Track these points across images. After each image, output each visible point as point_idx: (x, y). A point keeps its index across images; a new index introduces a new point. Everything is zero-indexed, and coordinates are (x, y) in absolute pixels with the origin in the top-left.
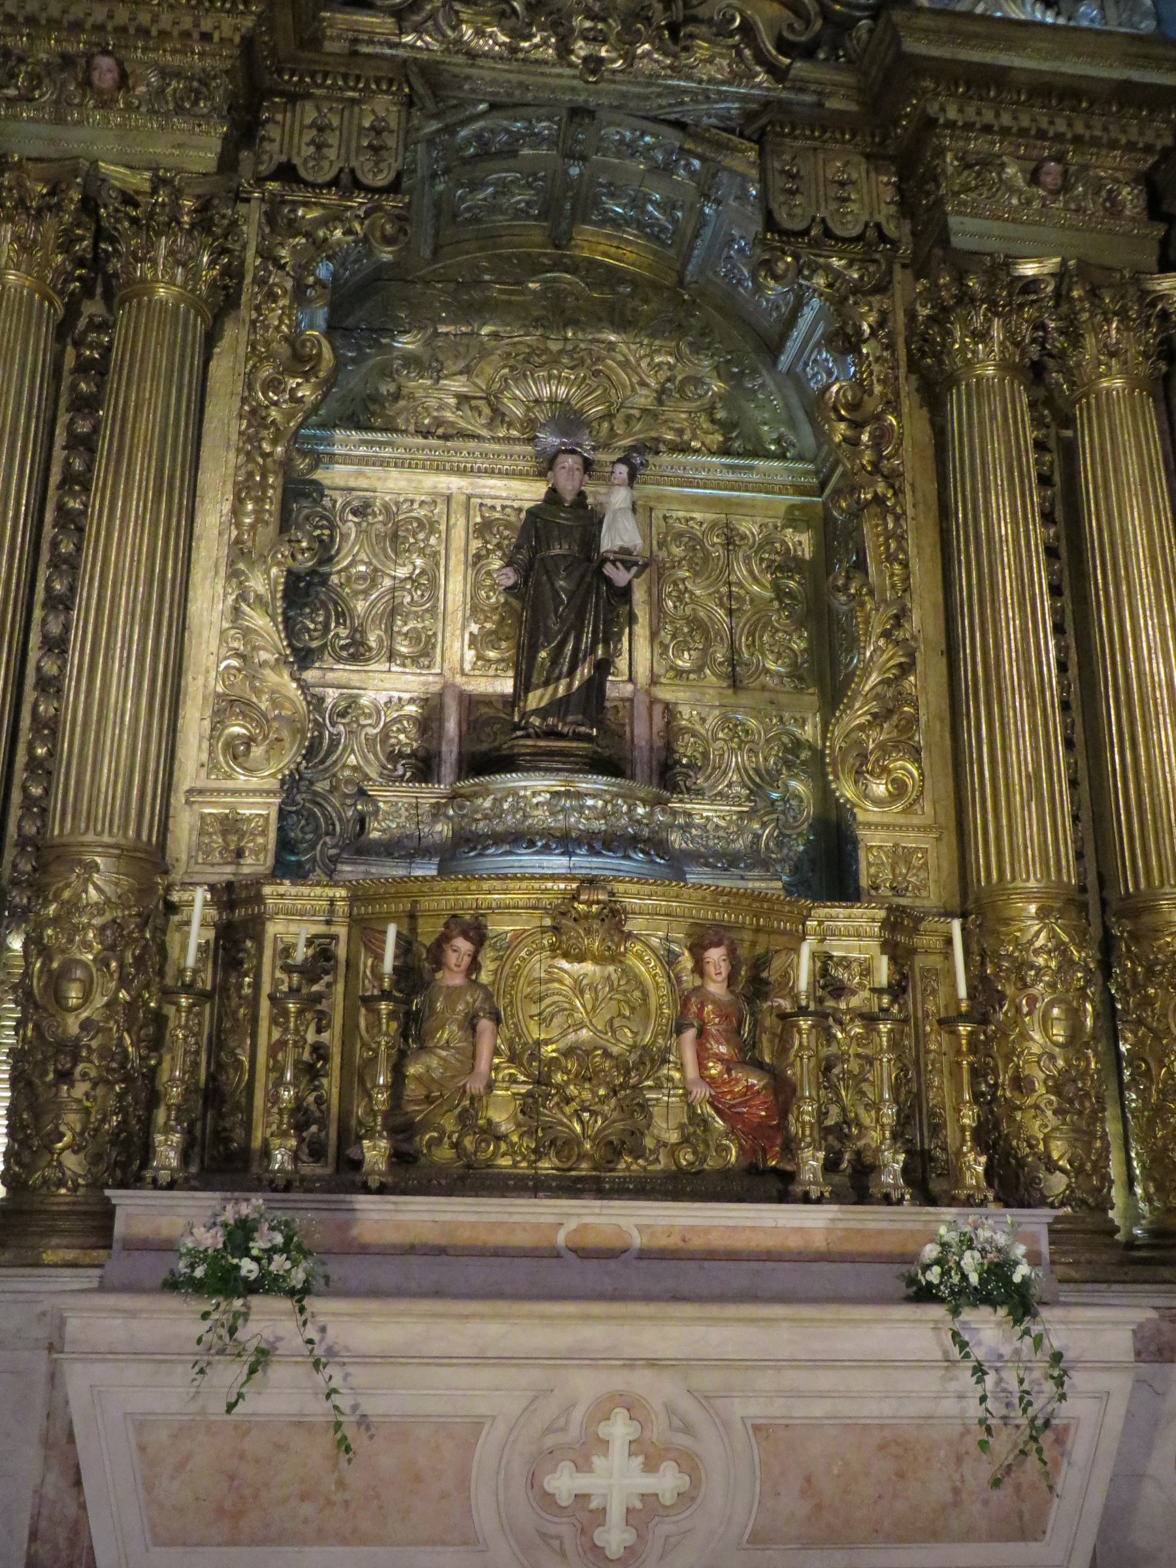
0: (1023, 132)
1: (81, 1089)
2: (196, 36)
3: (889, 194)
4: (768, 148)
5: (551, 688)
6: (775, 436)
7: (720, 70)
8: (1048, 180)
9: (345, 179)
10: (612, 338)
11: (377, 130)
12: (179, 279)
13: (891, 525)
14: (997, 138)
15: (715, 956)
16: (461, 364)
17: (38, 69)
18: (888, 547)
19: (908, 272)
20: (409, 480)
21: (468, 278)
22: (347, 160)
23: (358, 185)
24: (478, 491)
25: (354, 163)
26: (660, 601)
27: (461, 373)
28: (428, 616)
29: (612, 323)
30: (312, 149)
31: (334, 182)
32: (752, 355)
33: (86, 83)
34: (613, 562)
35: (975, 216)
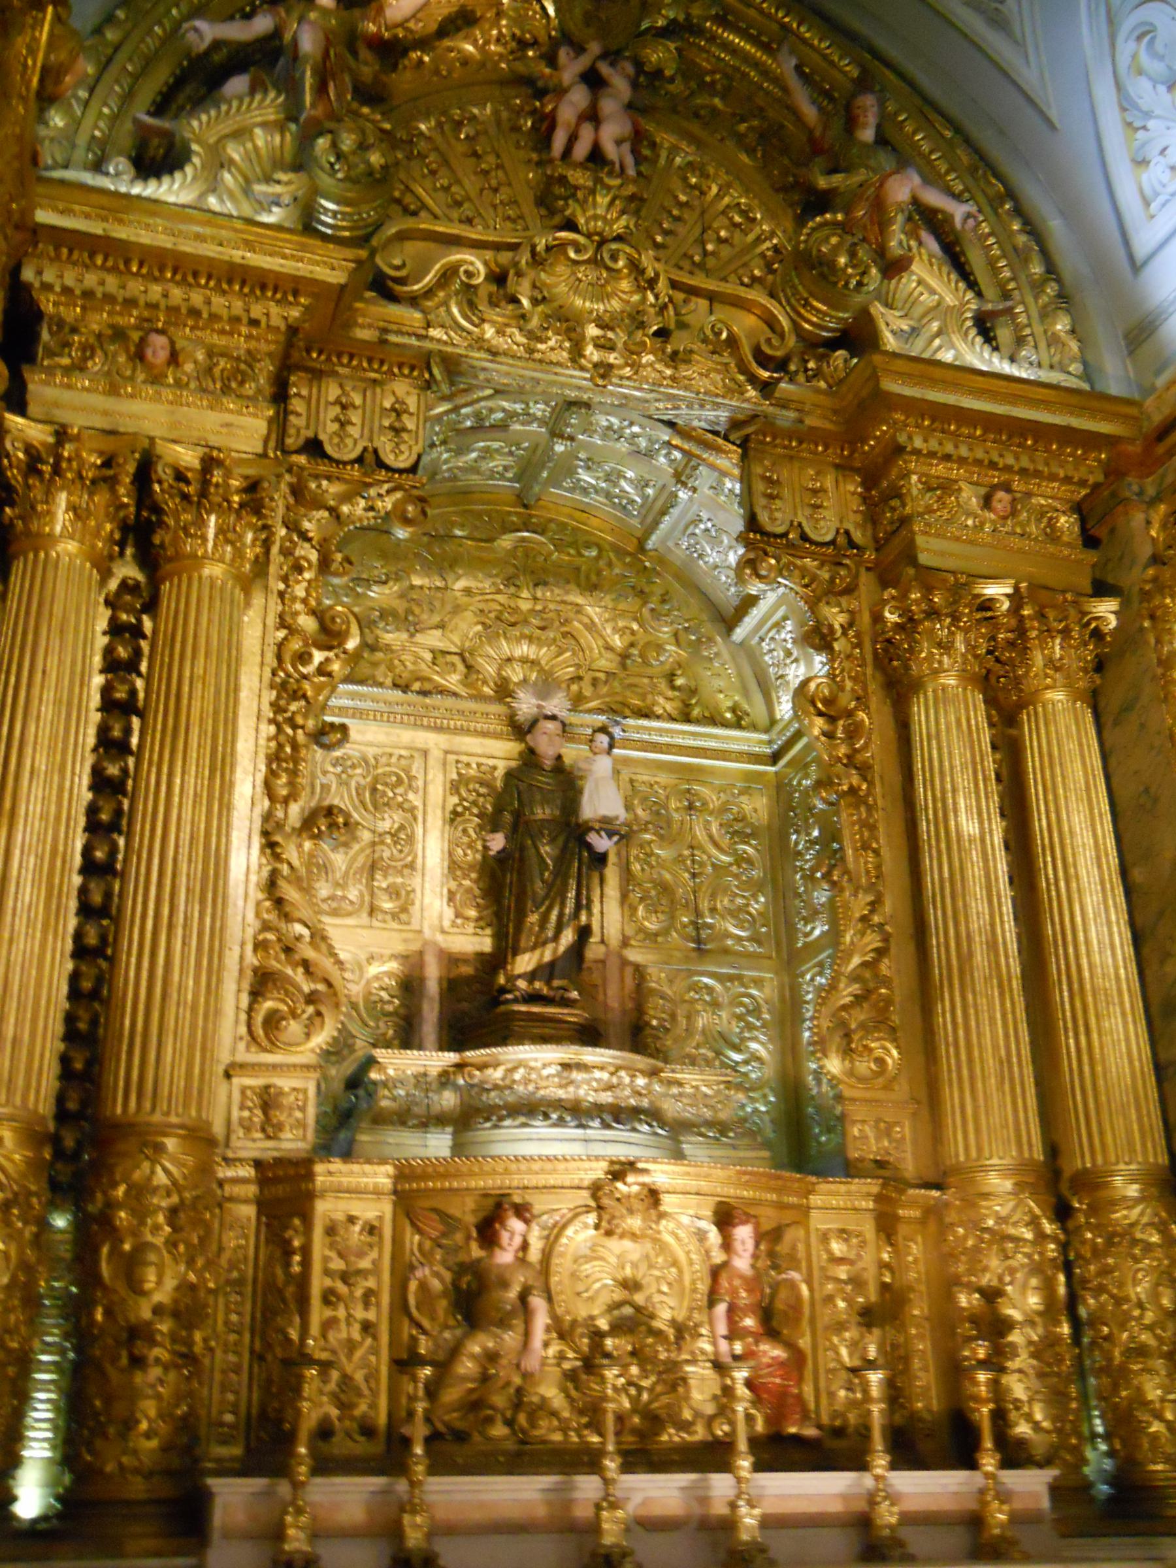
0: (978, 462)
1: (155, 1372)
2: (245, 320)
3: (855, 504)
4: (751, 453)
5: (537, 952)
6: (729, 704)
7: (714, 383)
8: (999, 506)
9: (370, 457)
10: (580, 600)
11: (398, 411)
12: (228, 557)
13: (864, 815)
14: (955, 466)
15: (743, 1234)
16: (436, 619)
17: (92, 340)
18: (862, 836)
19: (871, 574)
20: (388, 734)
21: (442, 532)
22: (371, 440)
23: (381, 464)
24: (455, 748)
25: (376, 444)
26: (628, 863)
27: (437, 627)
28: (406, 871)
29: (579, 585)
30: (336, 426)
31: (360, 460)
32: (709, 625)
33: (139, 356)
34: (598, 832)
35: (938, 535)
